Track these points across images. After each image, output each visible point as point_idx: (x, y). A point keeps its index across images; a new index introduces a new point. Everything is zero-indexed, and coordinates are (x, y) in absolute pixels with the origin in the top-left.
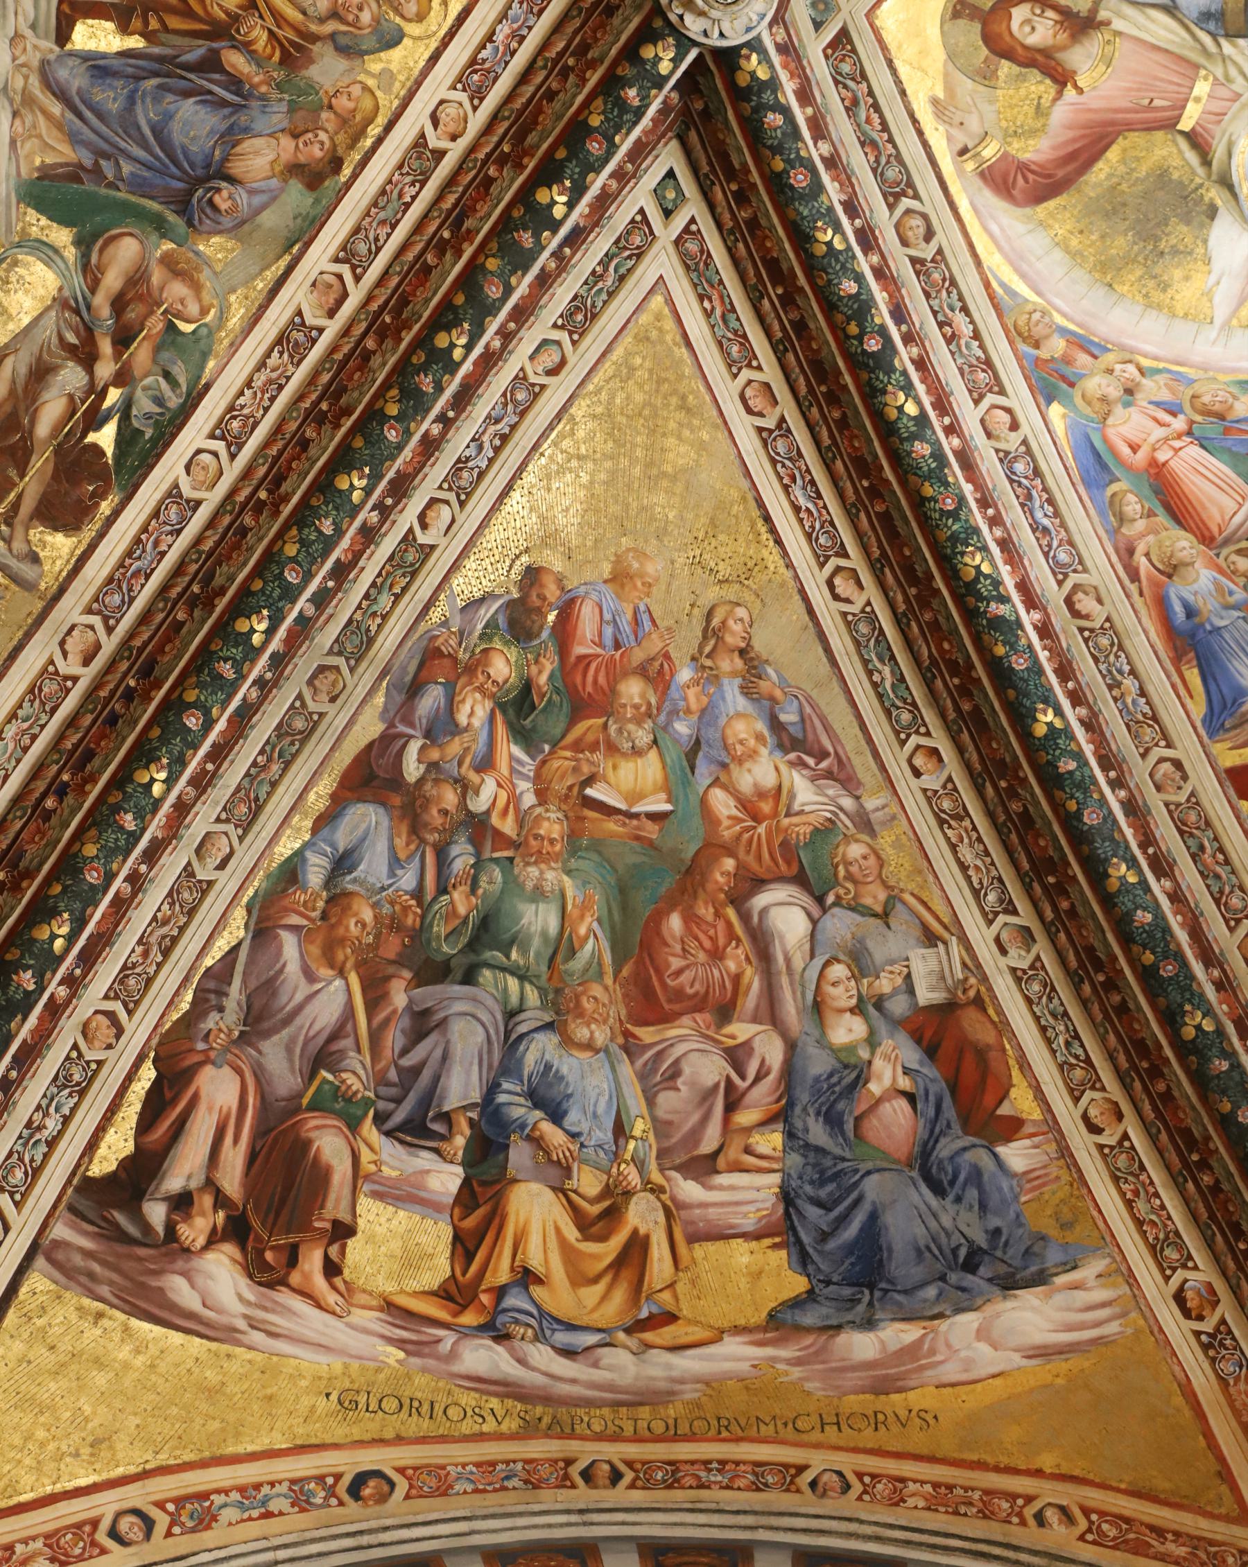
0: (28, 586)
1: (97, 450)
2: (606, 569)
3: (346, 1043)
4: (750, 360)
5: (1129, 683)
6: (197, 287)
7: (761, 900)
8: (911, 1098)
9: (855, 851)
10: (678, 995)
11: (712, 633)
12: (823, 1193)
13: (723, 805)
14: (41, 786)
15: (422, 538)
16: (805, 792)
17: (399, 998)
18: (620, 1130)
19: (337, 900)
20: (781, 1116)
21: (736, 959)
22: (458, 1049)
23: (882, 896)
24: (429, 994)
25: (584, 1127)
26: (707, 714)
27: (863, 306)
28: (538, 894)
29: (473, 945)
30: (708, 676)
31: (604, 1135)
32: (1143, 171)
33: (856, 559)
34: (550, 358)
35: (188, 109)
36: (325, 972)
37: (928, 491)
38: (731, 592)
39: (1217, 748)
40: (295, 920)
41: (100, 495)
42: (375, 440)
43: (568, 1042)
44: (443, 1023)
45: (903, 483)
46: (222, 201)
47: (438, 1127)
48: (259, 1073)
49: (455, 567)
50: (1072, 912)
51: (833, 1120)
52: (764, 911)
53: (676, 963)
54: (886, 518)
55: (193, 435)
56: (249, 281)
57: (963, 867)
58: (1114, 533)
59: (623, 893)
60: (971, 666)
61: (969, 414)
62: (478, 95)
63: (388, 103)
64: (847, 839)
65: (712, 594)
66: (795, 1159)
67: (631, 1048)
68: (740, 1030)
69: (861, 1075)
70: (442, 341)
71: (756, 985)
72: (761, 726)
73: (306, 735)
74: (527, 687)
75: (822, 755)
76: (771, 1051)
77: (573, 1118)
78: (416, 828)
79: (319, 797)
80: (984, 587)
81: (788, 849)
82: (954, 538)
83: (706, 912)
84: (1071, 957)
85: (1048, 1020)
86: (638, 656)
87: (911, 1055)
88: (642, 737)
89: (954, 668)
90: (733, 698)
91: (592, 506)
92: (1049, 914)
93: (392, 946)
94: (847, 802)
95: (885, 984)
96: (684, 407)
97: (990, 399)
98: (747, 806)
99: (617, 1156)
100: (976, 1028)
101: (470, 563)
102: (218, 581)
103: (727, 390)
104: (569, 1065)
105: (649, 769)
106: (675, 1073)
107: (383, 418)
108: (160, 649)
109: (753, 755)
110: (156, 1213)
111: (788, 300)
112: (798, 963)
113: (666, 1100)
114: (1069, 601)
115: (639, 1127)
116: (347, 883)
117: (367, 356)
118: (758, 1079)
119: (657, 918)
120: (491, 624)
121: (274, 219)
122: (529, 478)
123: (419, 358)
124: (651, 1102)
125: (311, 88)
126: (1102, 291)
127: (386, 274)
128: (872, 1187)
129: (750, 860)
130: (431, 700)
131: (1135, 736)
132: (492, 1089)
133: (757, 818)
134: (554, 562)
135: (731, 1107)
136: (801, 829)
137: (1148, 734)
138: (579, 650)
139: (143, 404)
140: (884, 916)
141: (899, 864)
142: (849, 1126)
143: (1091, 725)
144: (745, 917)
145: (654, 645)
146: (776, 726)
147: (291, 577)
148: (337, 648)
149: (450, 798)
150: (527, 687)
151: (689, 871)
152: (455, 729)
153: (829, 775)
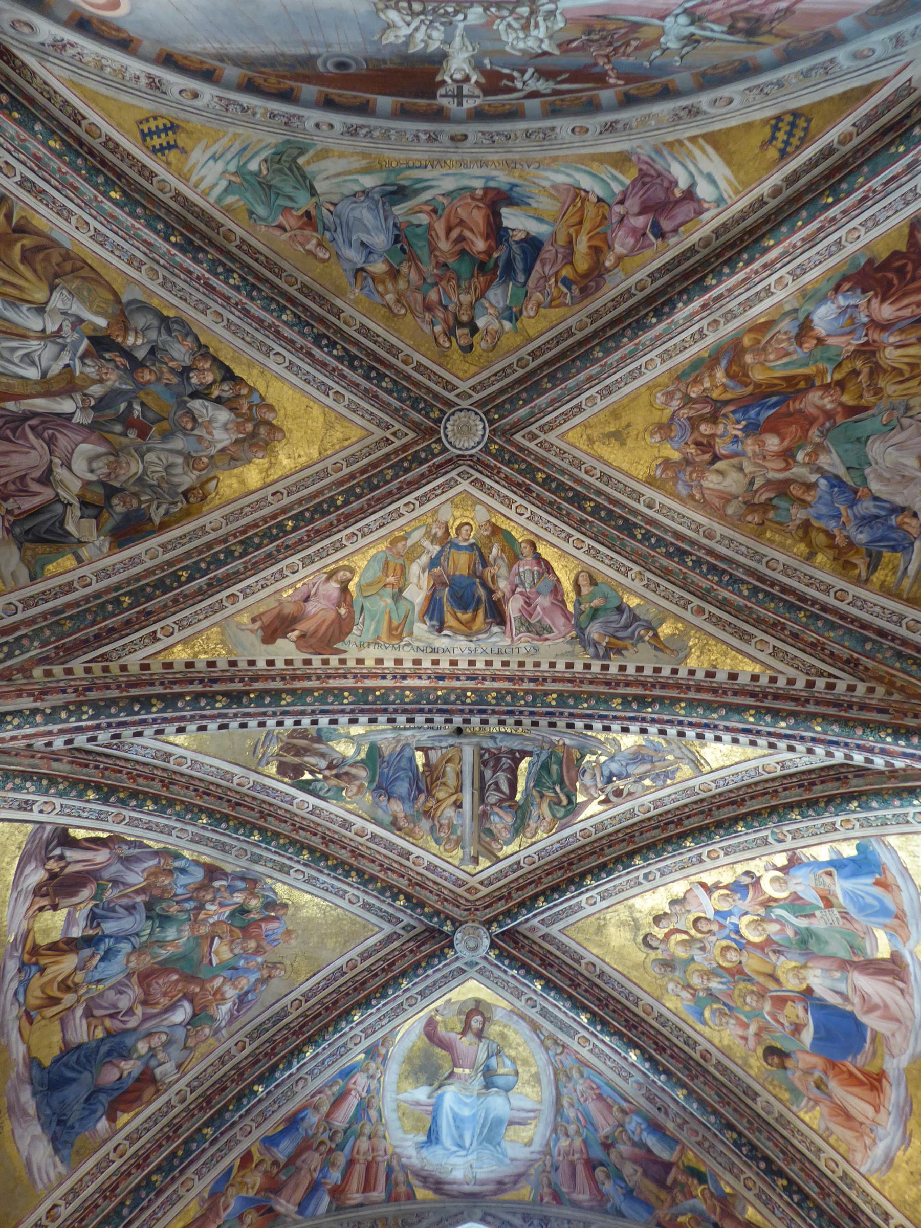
0: (259, 764)
1: (303, 774)
2: (290, 928)
3: (122, 887)
4: (364, 960)
5: (276, 1106)
6: (356, 794)
7: (186, 1004)
8: (120, 1078)
9: (207, 1031)
10: (149, 985)
11: (275, 966)
12: (83, 1059)
13: (218, 982)
14: (197, 783)
15: (292, 871)
16: (225, 1008)
17: (139, 899)
18: (99, 981)
19: (170, 872)
20: (109, 1034)
21: (165, 1001)
22: (122, 922)
23: (192, 1045)
24: (142, 908)
25: (99, 969)
26: (247, 970)
27: (383, 996)
28: (179, 931)
29: (160, 916)
30: (260, 968)
31: (97, 976)
32: (440, 1062)
33: (306, 1006)
34: (354, 900)
35: (406, 785)
36: (145, 875)
37: (330, 1029)
38: (289, 968)
39: (257, 1143)
40: (162, 861)
41: (290, 778)
42: (319, 859)
43: (129, 955)
44: (131, 914)
45: (332, 1020)
46: (382, 798)
47: (95, 924)
48: (110, 865)
49: (284, 883)
50: (193, 1116)
51: (109, 1053)
52: (182, 1006)
53: (161, 981)
54: (320, 1014)
55: (312, 800)
56: (360, 808)
57: (205, 1070)
58: (326, 1085)
59: (183, 957)
60: (275, 1055)
61: (357, 1031)
62: (427, 869)
63: (420, 843)
64: (211, 1027)
65: (288, 963)
66: (94, 1044)
67: (129, 976)
68: (139, 1010)
69: (126, 1057)
70: (353, 874)
71: (155, 1011)
72: (246, 988)
73: (224, 851)
74: (248, 912)
75: (238, 1011)
76: (132, 1023)
77: (102, 964)
78: (198, 889)
79: (204, 859)
80: (302, 1055)
81: (204, 1008)
82: (316, 1041)
83: (180, 987)
84: (177, 1120)
85: (154, 1118)
86: (264, 943)
87: (136, 1073)
88: (237, 951)
89: (273, 1049)
90: (253, 978)
91: (310, 920)
92: (192, 1107)
93: (156, 892)
94: (223, 1024)
95: (161, 1056)
96: (346, 942)
97: (363, 1035)
98: (218, 991)
99: (90, 983)
100: (149, 1092)
101: (286, 887)
102: (269, 818)
103: (353, 954)
104: (121, 958)
105: (226, 955)
106: (121, 993)
107: (327, 860)
108: (245, 806)
109: (236, 988)
110: (58, 852)
111: (383, 970)
112: (165, 1023)
113: (111, 993)
114: (301, 1078)
115: (101, 987)
116: (176, 874)
117: (345, 848)
118: (122, 1022)
119: (175, 971)
120: (268, 897)
121: (380, 813)
122: (316, 900)
123: (347, 868)
124: (110, 988)
125: (420, 820)
126: (401, 1059)
127: (370, 849)
128: (87, 1075)
129: (200, 996)
130: (240, 884)
131: (258, 1115)
132: (110, 937)
133: (215, 994)
134: (291, 911)
135: (112, 1016)
136: (211, 1011)
137: (260, 1119)
138: (263, 925)
139: (319, 785)
140: (185, 1048)
141: (202, 1049)
142: (108, 1059)
143: (260, 1101)
144: (179, 1000)
145: (268, 948)
146: (246, 993)
147: (273, 843)
148: (253, 854)
149: (209, 897)
150: (248, 912)
151: (193, 977)
152: (232, 894)
153: (232, 1015)
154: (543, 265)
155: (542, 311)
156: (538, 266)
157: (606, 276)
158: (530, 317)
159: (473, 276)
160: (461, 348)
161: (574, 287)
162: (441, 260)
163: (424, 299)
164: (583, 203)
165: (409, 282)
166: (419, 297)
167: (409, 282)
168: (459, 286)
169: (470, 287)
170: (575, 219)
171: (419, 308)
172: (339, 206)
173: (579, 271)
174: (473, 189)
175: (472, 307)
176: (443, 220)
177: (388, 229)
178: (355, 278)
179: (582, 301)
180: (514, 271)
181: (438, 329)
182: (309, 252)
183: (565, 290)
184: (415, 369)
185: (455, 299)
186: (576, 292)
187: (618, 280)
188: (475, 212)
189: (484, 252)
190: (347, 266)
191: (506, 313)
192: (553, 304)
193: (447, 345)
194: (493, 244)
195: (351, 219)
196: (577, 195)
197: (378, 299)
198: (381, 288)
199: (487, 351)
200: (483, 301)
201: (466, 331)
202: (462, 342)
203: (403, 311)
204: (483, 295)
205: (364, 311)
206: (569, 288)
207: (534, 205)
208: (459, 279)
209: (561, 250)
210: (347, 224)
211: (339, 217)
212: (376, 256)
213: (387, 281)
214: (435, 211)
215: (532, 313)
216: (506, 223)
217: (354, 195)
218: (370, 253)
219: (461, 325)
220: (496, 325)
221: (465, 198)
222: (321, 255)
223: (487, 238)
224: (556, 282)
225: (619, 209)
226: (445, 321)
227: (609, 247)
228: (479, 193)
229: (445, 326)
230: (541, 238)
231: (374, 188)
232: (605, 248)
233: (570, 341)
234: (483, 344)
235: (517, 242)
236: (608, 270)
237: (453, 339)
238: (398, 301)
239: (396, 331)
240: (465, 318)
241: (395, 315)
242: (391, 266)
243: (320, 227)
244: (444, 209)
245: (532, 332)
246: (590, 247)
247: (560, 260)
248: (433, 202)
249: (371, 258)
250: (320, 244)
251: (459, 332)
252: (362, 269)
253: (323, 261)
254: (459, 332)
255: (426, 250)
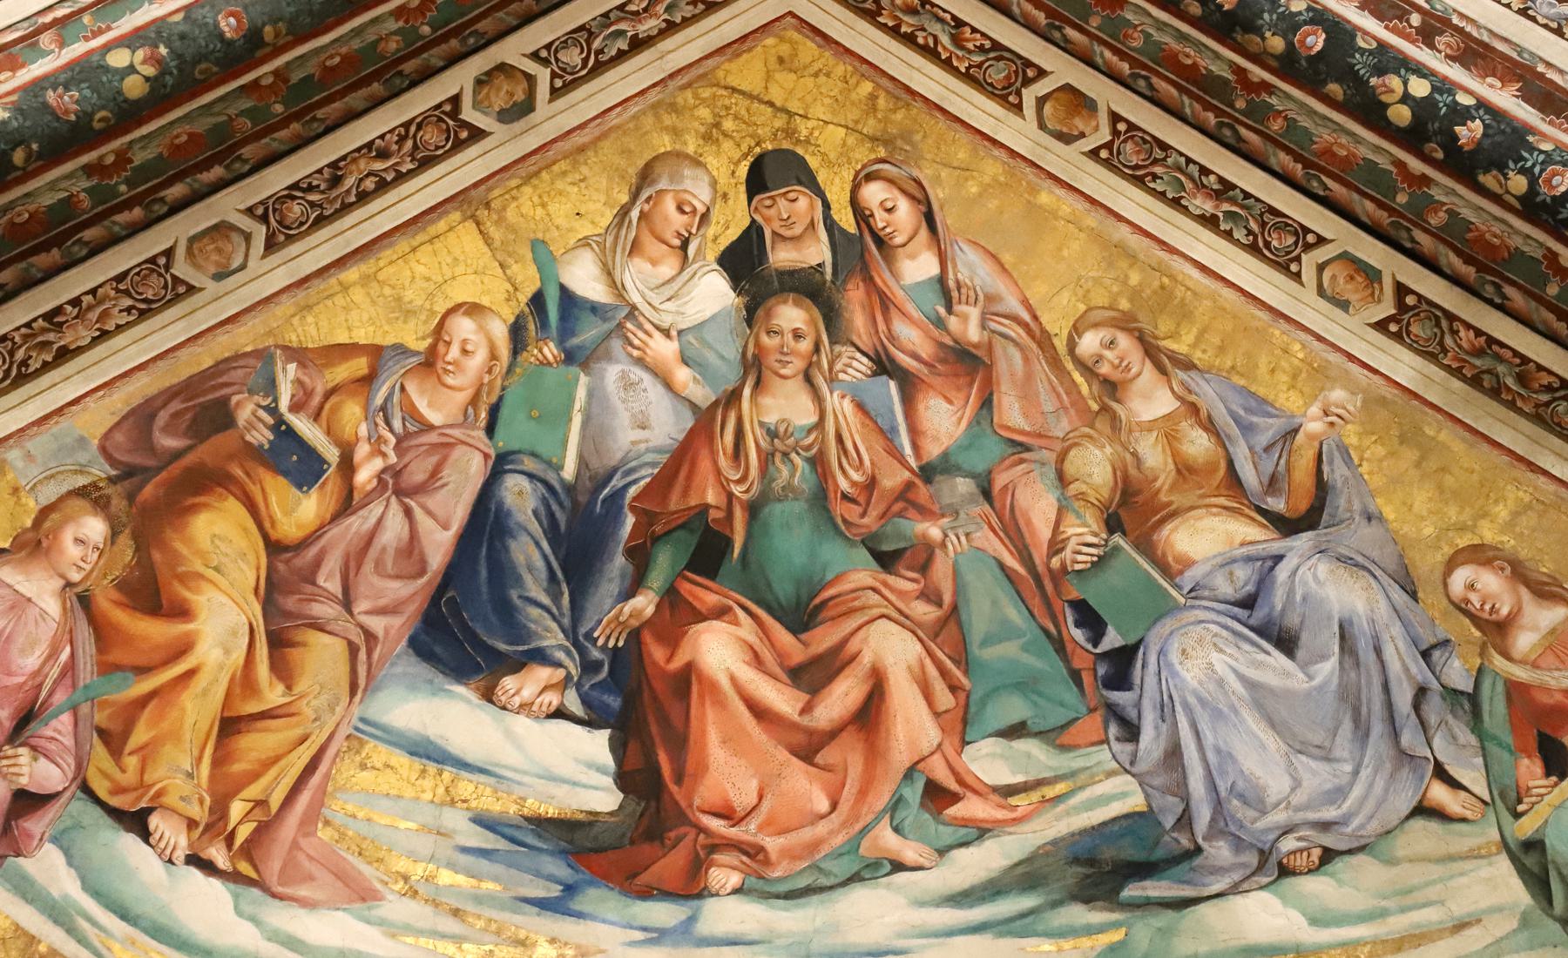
154: (412, 548)
155: (414, 337)
156: (439, 544)
157: (101, 470)
158: (473, 309)
159: (754, 510)
160: (808, 180)
161: (261, 436)
162: (906, 582)
163: (987, 403)
164: (220, 810)
165: (1062, 480)
166: (1011, 412)
167: (1062, 480)
168: (818, 462)
169: (766, 459)
170: (255, 744)
171: (1009, 362)
172: (1404, 801)
173: (234, 506)
174: (755, 889)
175: (755, 368)
176: (900, 753)
177: (1165, 710)
178: (1322, 488)
179: (222, 366)
180: (552, 529)
181: (919, 267)
182: (1545, 592)
183: (303, 426)
184: (1029, 72)
185: (840, 406)
186: (246, 410)
187: (40, 443)
188: (743, 793)
189: (701, 617)
190: (1357, 538)
191: (588, 333)
192: (360, 365)
193: (874, 194)
194: (657, 653)
195: (1343, 745)
196: (249, 851)
197: (1208, 394)
198: (1198, 444)
199: (679, 155)
200: (703, 395)
201: (782, 257)
202: (803, 204)
203: (1089, 343)
204: (704, 423)
205: (1278, 331)
206: (285, 432)
207: (456, 820)
208: (821, 498)
209: (324, 610)
210: (1362, 732)
211: (1404, 757)
212: (1226, 589)
213: (1165, 478)
214: (937, 796)
215: (463, 327)
216: (597, 745)
217: (1328, 855)
218: (1248, 603)
219: (805, 285)
220: (639, 277)
221: (790, 854)
222: (1491, 582)
223: (687, 679)
224: (348, 466)
225: (44, 774)
226: (885, 303)
227: (85, 600)
228: (724, 875)
229: (882, 276)
230: (423, 670)
231: (1235, 890)
232: (105, 602)
233: (277, 179)
234: (701, 194)
235: (540, 657)
236: (91, 496)
237: (846, 220)
238: (1112, 388)
239: (1120, 247)
240: (791, 315)
241: (1125, 323)
242: (1146, 546)
243: (1495, 709)
244: (897, 803)
245: (463, 241)
246: (182, 612)
247: (332, 564)
248: (947, 834)
249: (1244, 576)
250: (1497, 630)
251: (818, 252)
252: (1287, 526)
253: (1479, 554)
254: (818, 252)
255: (978, 620)
